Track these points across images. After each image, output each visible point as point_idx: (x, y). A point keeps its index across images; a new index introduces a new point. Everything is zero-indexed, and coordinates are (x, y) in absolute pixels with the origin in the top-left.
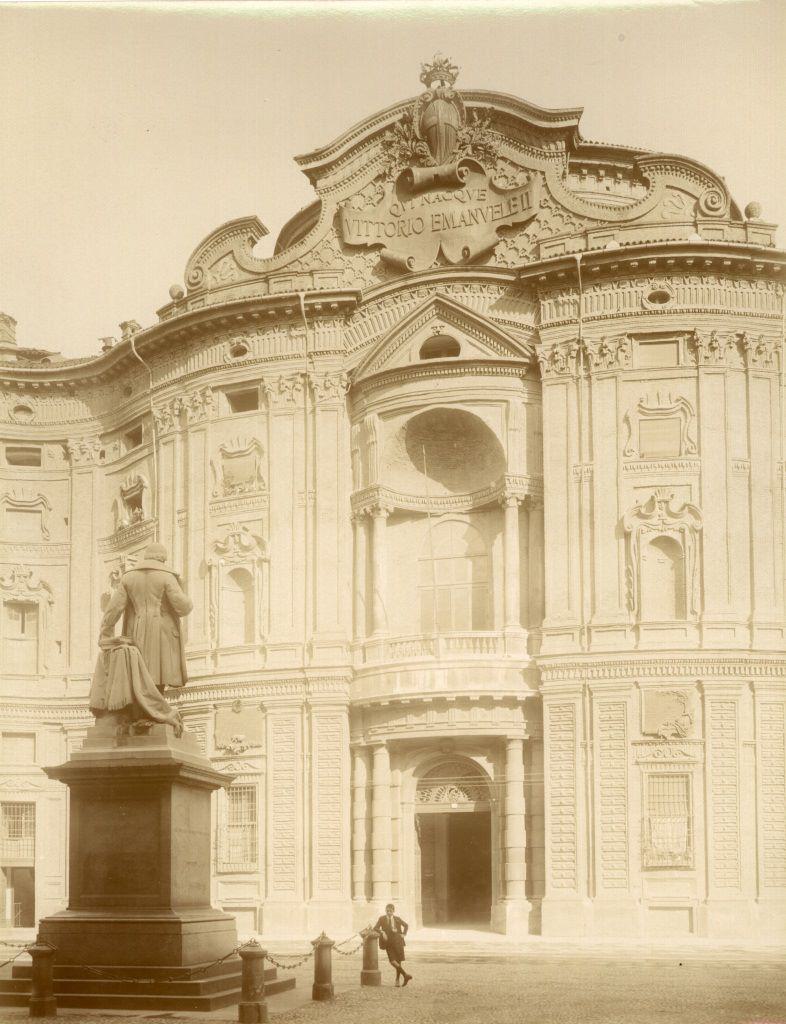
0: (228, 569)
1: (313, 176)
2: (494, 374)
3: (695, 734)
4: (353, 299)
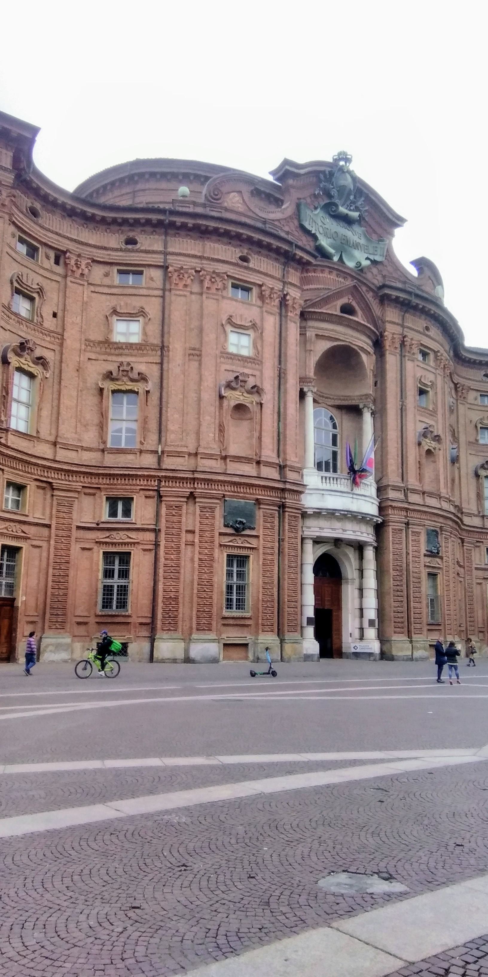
0: (233, 403)
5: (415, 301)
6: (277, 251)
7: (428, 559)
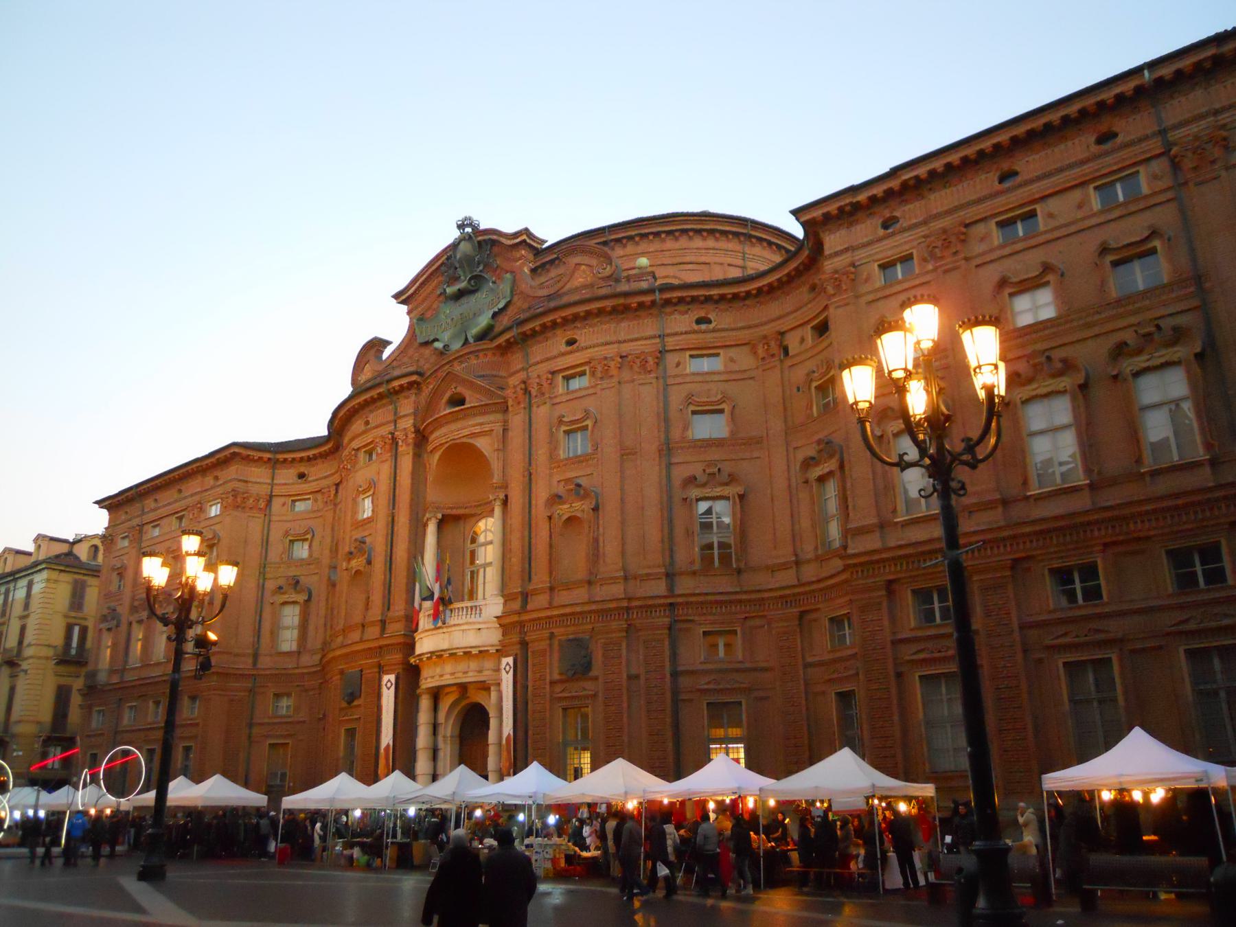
1: (403, 302)
2: (485, 413)
3: (594, 673)
4: (414, 378)
5: (527, 327)
6: (381, 396)
7: (558, 688)
